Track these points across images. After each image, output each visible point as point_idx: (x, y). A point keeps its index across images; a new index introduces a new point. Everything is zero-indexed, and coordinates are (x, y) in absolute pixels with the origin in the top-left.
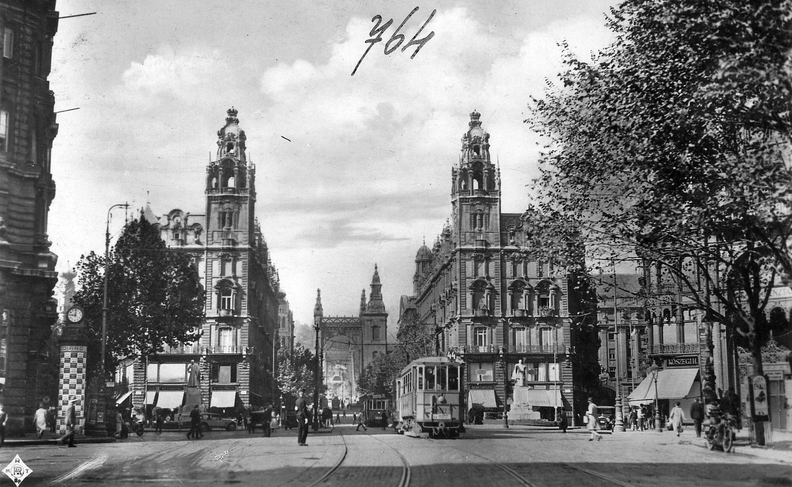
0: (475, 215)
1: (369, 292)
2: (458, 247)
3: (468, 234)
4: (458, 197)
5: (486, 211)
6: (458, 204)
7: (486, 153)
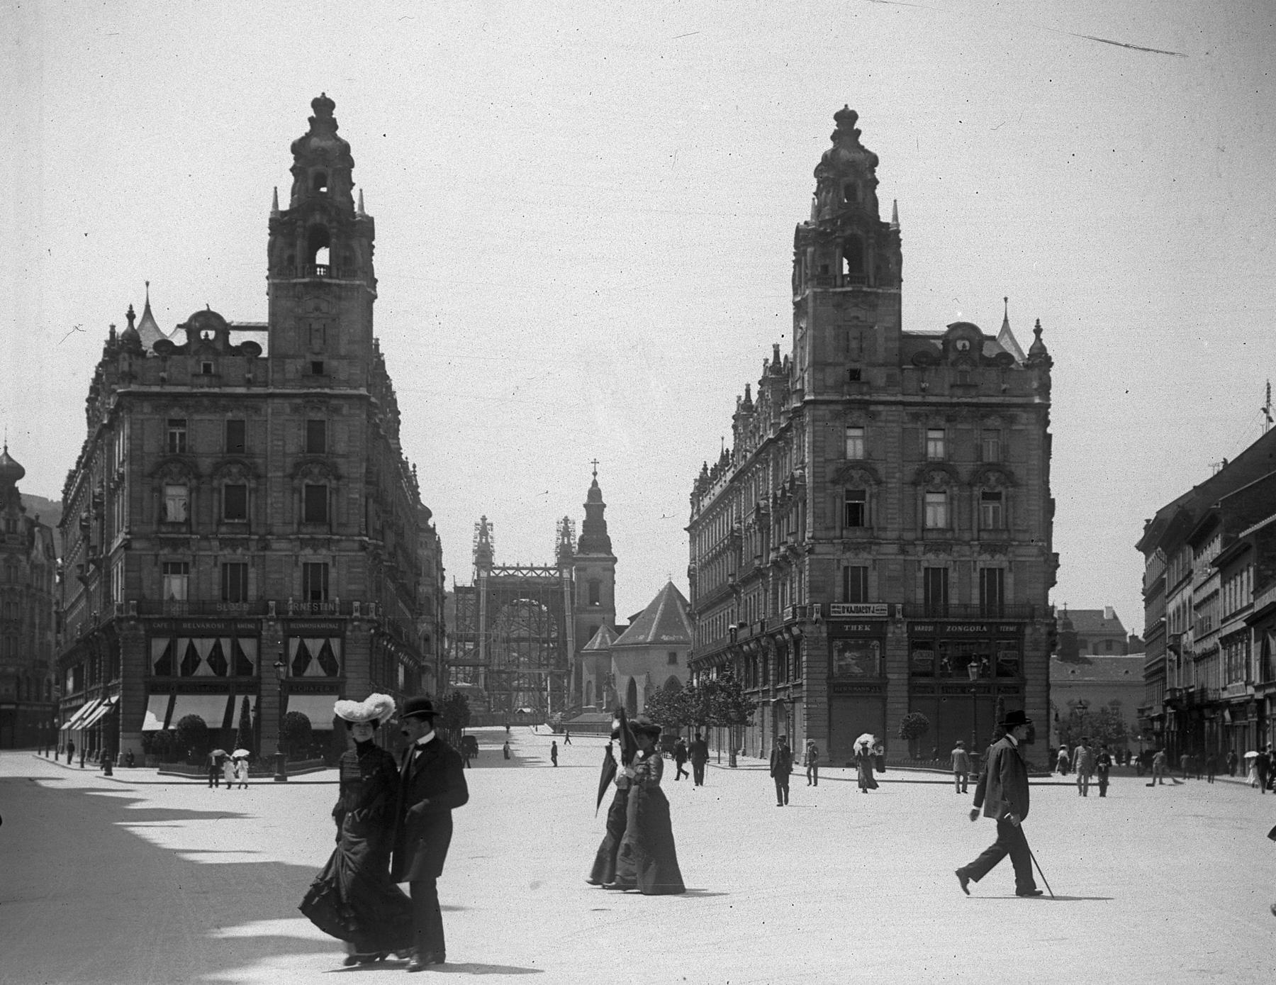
1: (579, 517)
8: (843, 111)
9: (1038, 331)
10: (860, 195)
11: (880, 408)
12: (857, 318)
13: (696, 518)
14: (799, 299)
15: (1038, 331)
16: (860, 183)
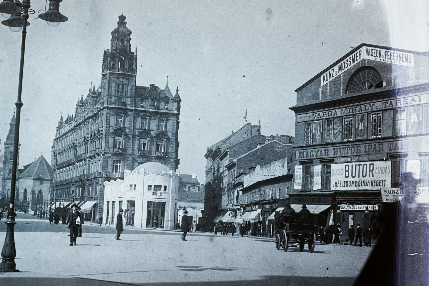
0: (119, 85)
2: (105, 105)
3: (113, 97)
4: (108, 72)
5: (126, 83)
6: (107, 76)
7: (128, 44)
8: (121, 16)
9: (177, 90)
10: (125, 43)
11: (128, 111)
12: (122, 82)
13: (58, 136)
14: (104, 73)
15: (177, 90)
16: (125, 38)
